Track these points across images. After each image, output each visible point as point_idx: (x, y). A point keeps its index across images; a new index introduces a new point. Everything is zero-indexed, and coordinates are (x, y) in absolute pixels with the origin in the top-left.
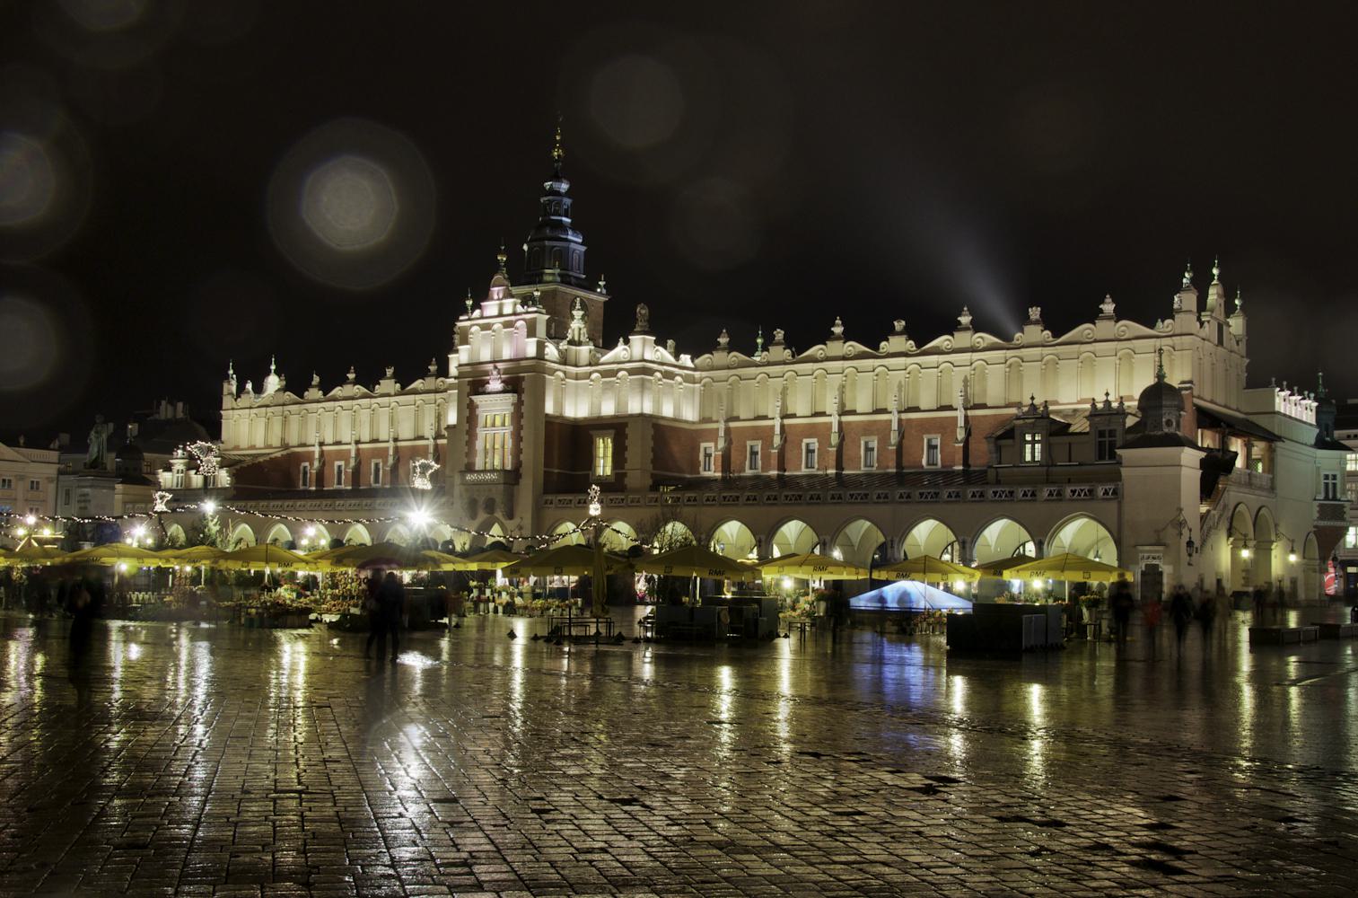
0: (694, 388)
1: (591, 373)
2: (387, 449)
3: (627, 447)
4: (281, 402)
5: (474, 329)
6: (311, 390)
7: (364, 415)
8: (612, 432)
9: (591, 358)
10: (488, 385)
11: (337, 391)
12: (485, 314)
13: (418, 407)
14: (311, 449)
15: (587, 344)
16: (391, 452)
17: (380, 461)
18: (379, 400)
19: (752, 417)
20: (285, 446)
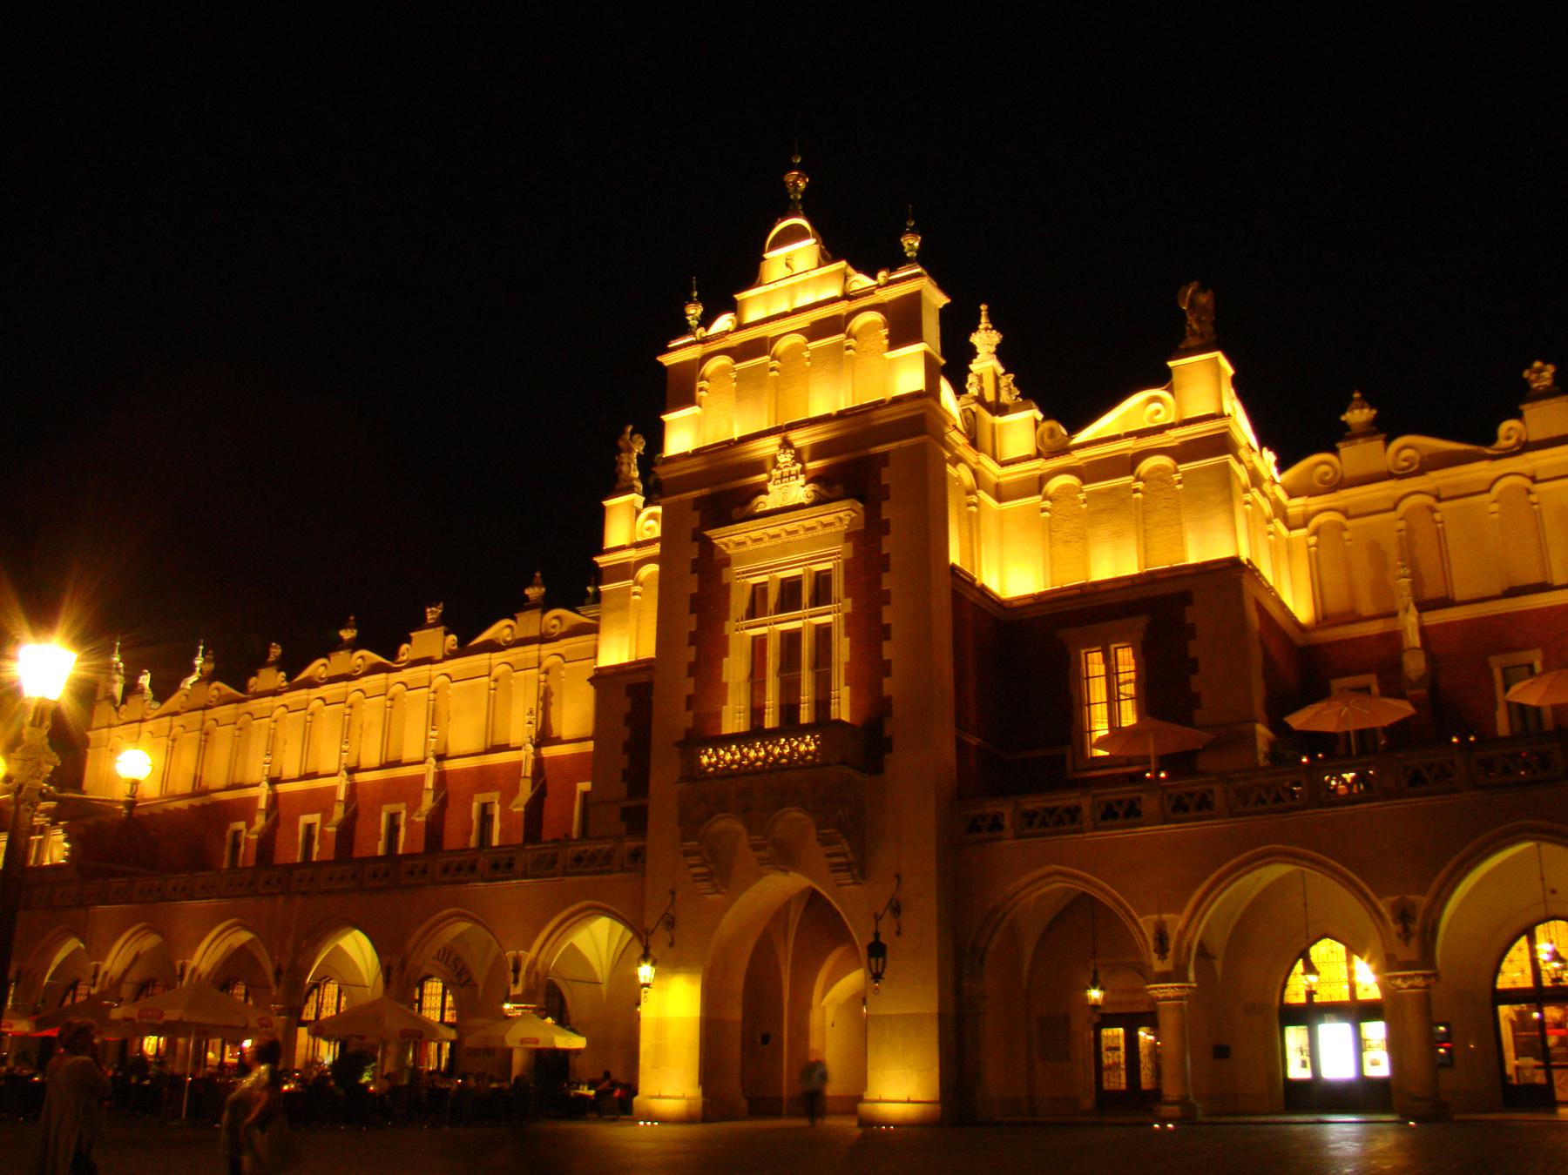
0: (1288, 542)
1: (1042, 480)
2: (420, 779)
3: (1195, 661)
4: (202, 702)
5: (711, 366)
6: (263, 672)
7: (372, 712)
8: (1141, 622)
9: (1040, 440)
10: (762, 498)
11: (317, 668)
12: (751, 315)
13: (496, 680)
14: (252, 792)
15: (1017, 408)
16: (429, 784)
17: (402, 809)
18: (408, 674)
19: (1498, 592)
20: (199, 790)
